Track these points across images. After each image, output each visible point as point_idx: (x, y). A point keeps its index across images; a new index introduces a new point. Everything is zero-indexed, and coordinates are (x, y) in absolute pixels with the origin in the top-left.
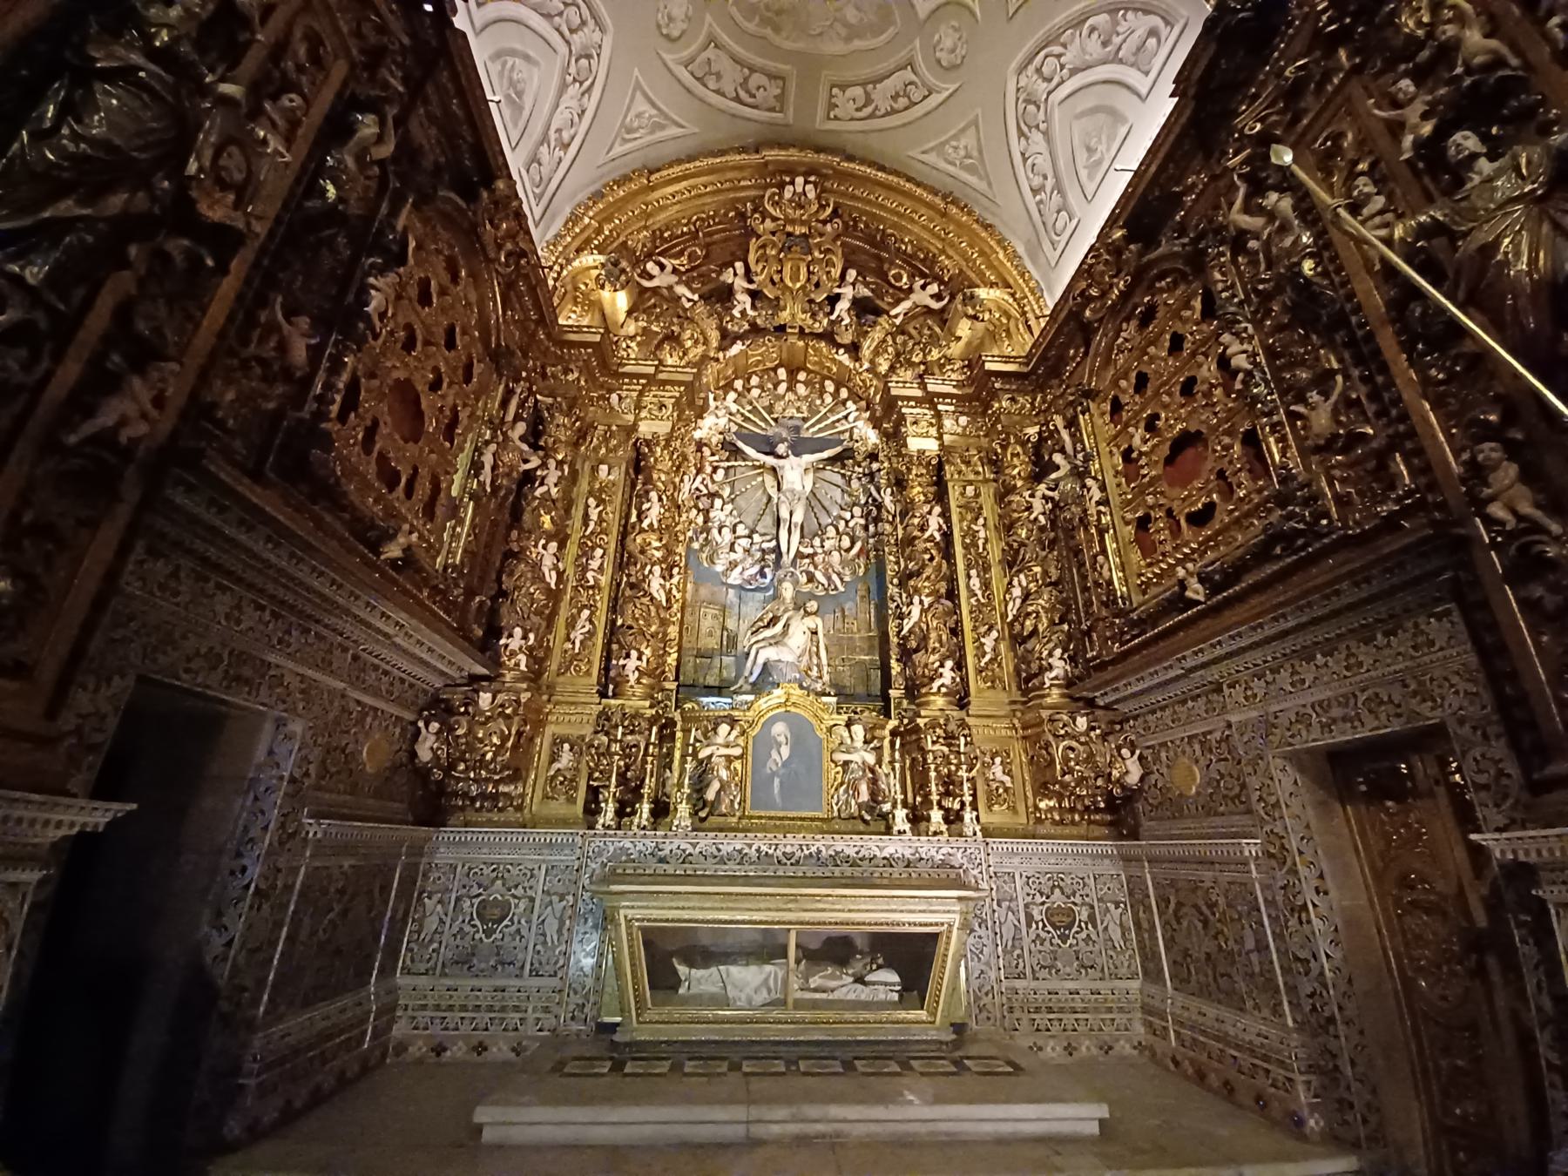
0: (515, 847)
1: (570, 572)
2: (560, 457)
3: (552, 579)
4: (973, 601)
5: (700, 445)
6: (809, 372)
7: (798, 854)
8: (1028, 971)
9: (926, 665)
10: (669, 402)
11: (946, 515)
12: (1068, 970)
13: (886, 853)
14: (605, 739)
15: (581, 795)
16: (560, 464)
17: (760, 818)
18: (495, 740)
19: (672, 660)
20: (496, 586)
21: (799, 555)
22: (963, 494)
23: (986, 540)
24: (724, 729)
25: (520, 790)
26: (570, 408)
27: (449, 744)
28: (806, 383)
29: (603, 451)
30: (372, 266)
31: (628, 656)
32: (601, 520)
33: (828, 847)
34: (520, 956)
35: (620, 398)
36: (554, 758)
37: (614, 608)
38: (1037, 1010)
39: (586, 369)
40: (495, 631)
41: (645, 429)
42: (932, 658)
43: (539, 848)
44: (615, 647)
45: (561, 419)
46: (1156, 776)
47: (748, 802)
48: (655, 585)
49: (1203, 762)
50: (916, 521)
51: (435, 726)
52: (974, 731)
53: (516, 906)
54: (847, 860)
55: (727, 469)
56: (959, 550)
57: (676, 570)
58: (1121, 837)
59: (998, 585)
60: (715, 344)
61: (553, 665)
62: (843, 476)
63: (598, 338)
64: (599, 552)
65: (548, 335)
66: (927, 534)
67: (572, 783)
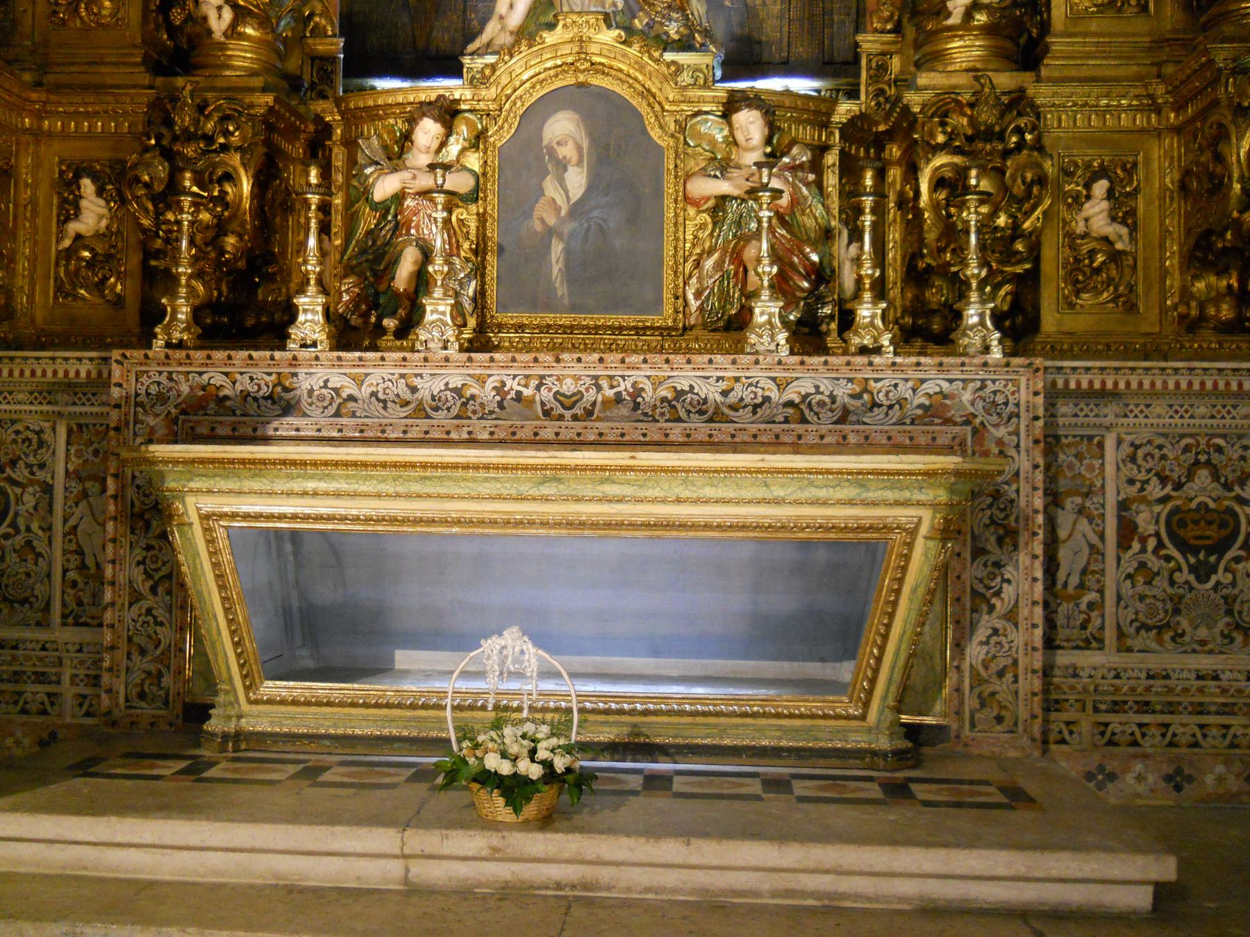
7: (590, 396)
8: (1110, 636)
12: (1203, 633)
13: (791, 394)
17: (520, 328)
24: (428, 130)
33: (657, 383)
34: (39, 590)
38: (1117, 707)
53: (19, 500)
54: (702, 408)
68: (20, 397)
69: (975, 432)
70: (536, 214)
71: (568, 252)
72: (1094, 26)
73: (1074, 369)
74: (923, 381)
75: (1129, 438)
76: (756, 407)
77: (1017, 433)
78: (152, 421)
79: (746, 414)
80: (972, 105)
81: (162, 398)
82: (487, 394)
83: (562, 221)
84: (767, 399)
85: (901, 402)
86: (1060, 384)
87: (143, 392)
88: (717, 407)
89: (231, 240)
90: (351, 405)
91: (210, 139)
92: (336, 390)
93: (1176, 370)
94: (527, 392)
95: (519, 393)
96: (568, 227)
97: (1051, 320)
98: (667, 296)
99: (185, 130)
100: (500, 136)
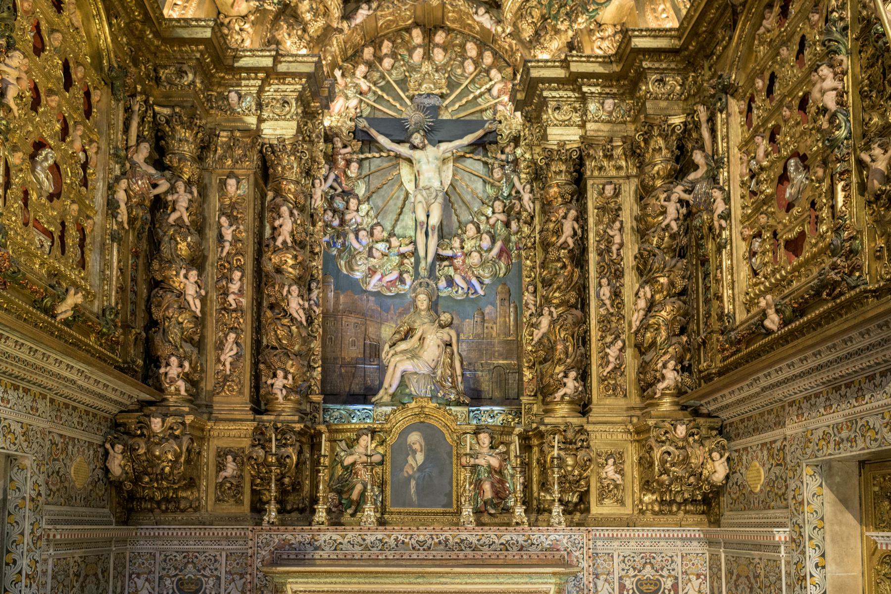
0: (199, 541)
2: (186, 177)
3: (196, 306)
5: (329, 137)
9: (551, 376)
10: (292, 97)
14: (261, 453)
15: (247, 498)
16: (189, 183)
17: (399, 513)
19: (317, 373)
21: (439, 258)
22: (601, 193)
23: (622, 245)
24: (365, 440)
25: (196, 494)
28: (445, 48)
31: (275, 376)
32: (236, 240)
35: (240, 97)
36: (221, 467)
37: (258, 328)
39: (201, 68)
40: (153, 361)
42: (559, 369)
43: (218, 541)
44: (262, 366)
45: (183, 133)
47: (389, 499)
48: (295, 305)
50: (551, 225)
52: (592, 436)
55: (360, 162)
56: (593, 257)
57: (314, 285)
59: (627, 294)
60: (336, 13)
61: (208, 385)
62: (486, 164)
63: (208, 34)
64: (237, 275)
66: (562, 240)
67: (237, 488)
71: (417, 484)
72: (608, 401)
80: (565, 431)
83: (415, 472)
89: (287, 480)
96: (417, 476)
98: (455, 502)
100: (391, 440)
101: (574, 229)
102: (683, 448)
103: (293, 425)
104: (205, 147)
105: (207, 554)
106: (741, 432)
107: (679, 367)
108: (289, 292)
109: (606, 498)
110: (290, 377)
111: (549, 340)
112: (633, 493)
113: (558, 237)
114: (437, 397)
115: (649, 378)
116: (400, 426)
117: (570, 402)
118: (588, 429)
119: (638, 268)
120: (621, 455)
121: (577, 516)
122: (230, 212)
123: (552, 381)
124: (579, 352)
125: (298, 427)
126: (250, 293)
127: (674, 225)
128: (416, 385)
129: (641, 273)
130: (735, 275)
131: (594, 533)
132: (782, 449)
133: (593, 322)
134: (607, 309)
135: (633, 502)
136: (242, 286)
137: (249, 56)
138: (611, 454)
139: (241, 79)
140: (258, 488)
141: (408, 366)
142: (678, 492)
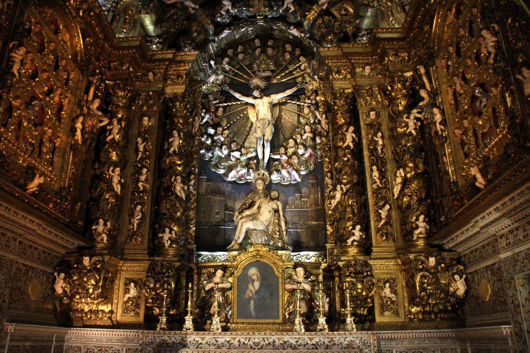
1: (130, 182)
3: (118, 189)
4: (374, 186)
6: (274, 39)
7: (262, 343)
9: (344, 229)
11: (357, 131)
13: (314, 342)
18: (93, 282)
20: (89, 195)
23: (383, 145)
24: (219, 273)
26: (125, 86)
27: (70, 285)
29: (145, 108)
30: (13, 47)
31: (164, 232)
32: (145, 150)
33: (279, 339)
36: (127, 291)
40: (91, 221)
41: (169, 90)
42: (349, 224)
44: (157, 226)
46: (473, 290)
48: (179, 188)
49: (492, 282)
51: (62, 275)
54: (291, 346)
56: (366, 153)
58: (459, 327)
59: (389, 175)
61: (121, 239)
64: (145, 170)
65: (111, 46)
68: (114, 341)
69: (360, 351)
70: (247, 293)
71: (255, 303)
73: (384, 333)
74: (346, 338)
75: (399, 350)
76: (305, 345)
77: (370, 350)
78: (149, 349)
79: (302, 347)
80: (355, 265)
81: (152, 343)
82: (236, 343)
83: (253, 295)
84: (307, 343)
85: (341, 343)
86: (381, 337)
87: (147, 341)
88: (295, 345)
90: (201, 345)
91: (164, 274)
92: (197, 341)
93: (409, 333)
94: (246, 342)
95: (244, 342)
96: (255, 297)
97: (379, 319)
98: (281, 315)
99: (158, 272)
100: (237, 273)
101: (353, 137)
102: (435, 273)
103: (174, 263)
104: (132, 100)
105: (113, 349)
106: (472, 260)
107: (427, 220)
108: (175, 180)
109: (386, 311)
110: (173, 232)
111: (342, 206)
112: (404, 306)
113: (344, 143)
114: (269, 245)
115: (408, 228)
116: (244, 263)
117: (357, 246)
118: (371, 264)
119: (395, 159)
120: (394, 280)
121: (367, 325)
122: (144, 134)
123: (345, 232)
124: (362, 214)
125: (178, 264)
126: (152, 182)
127: (414, 132)
128: (255, 237)
129: (397, 162)
130: (455, 158)
131: (378, 335)
132: (499, 269)
133: (370, 194)
134: (378, 185)
135: (405, 313)
136: (147, 177)
137: (160, 54)
138: (388, 280)
139: (156, 66)
140: (150, 305)
141: (250, 225)
142: (435, 304)
